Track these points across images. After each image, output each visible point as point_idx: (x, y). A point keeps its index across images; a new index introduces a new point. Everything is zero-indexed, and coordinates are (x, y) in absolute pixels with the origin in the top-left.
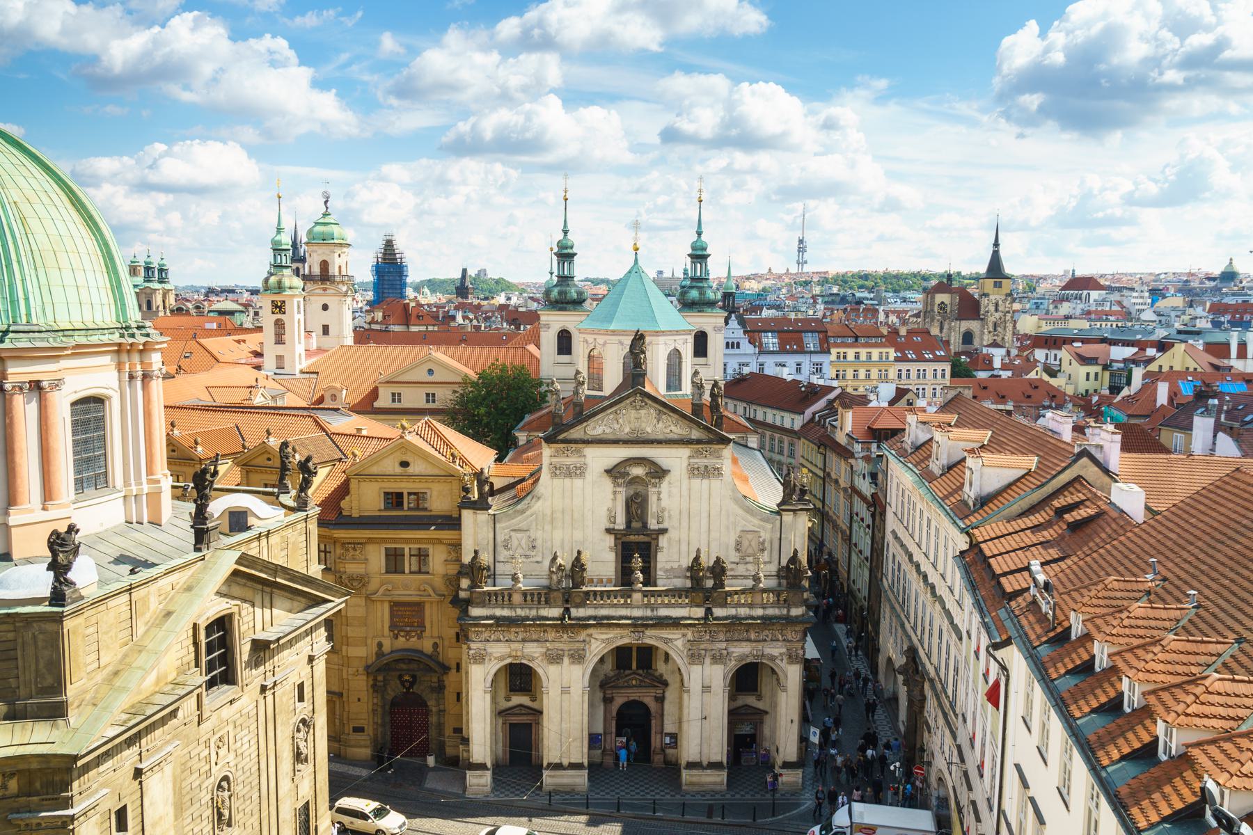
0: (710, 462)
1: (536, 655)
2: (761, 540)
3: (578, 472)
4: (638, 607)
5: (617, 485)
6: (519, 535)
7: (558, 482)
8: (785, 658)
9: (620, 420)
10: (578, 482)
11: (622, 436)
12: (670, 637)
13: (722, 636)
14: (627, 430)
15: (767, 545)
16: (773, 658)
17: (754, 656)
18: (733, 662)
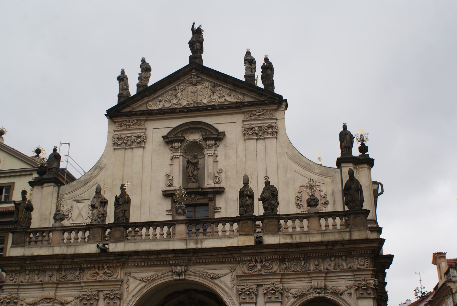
0: (265, 123)
1: (70, 299)
2: (322, 194)
3: (138, 140)
4: (181, 240)
5: (173, 149)
6: (81, 205)
7: (120, 153)
8: (352, 291)
9: (179, 95)
10: (139, 152)
11: (181, 107)
12: (217, 272)
13: (276, 267)
14: (185, 103)
15: (329, 198)
16: (338, 294)
17: (315, 288)
18: (293, 300)
